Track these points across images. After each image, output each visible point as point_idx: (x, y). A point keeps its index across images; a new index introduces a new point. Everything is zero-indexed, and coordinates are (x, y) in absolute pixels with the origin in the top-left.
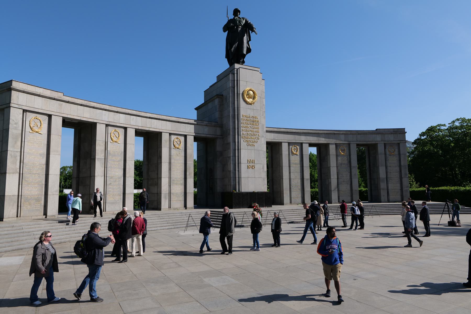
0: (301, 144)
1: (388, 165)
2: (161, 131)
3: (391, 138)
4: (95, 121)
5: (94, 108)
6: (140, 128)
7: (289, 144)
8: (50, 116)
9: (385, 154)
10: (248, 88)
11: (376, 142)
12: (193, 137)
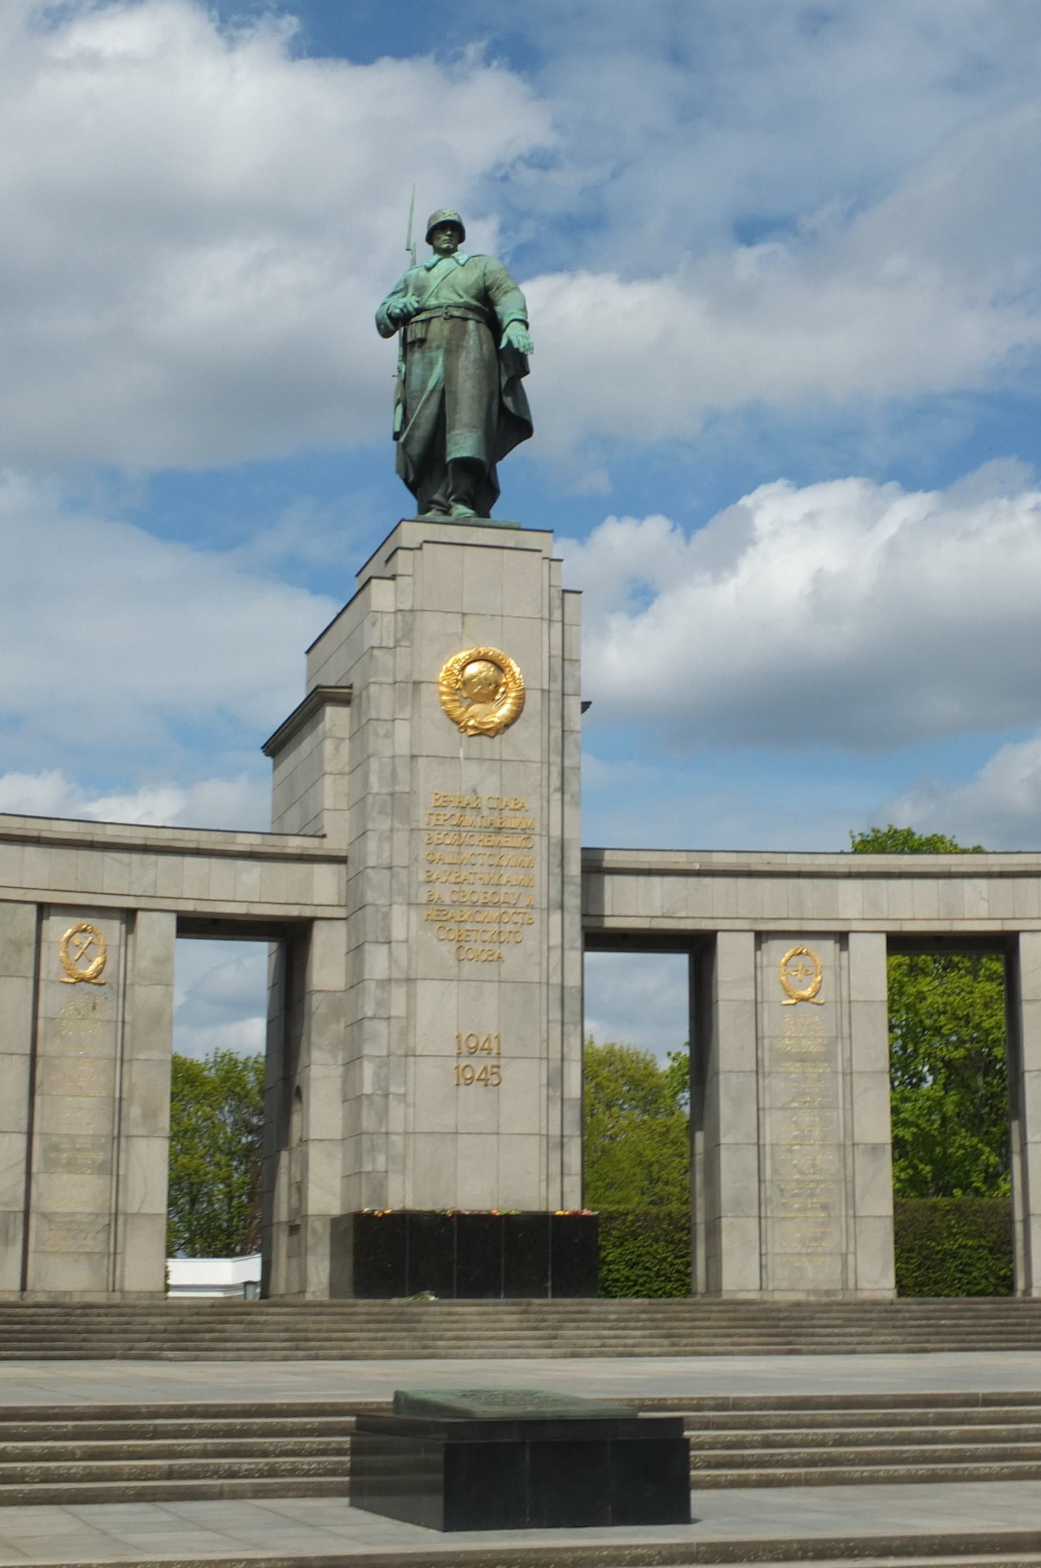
0: (842, 938)
7: (761, 937)
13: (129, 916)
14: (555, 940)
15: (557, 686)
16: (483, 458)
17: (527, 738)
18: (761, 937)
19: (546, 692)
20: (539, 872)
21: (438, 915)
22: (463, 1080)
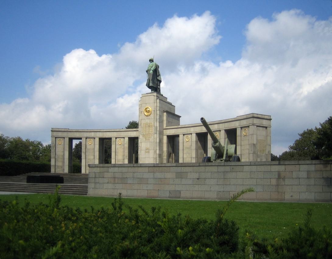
0: (191, 134)
1: (243, 144)
2: (111, 137)
3: (244, 123)
4: (81, 137)
5: (80, 132)
6: (101, 137)
7: (184, 135)
8: (64, 138)
9: (241, 136)
10: (146, 107)
11: (236, 127)
12: (127, 138)
13: (124, 138)
14: (155, 137)
15: (156, 110)
16: (153, 86)
17: (152, 116)
18: (184, 135)
19: (154, 111)
20: (153, 130)
21: (144, 136)
22: (146, 152)
